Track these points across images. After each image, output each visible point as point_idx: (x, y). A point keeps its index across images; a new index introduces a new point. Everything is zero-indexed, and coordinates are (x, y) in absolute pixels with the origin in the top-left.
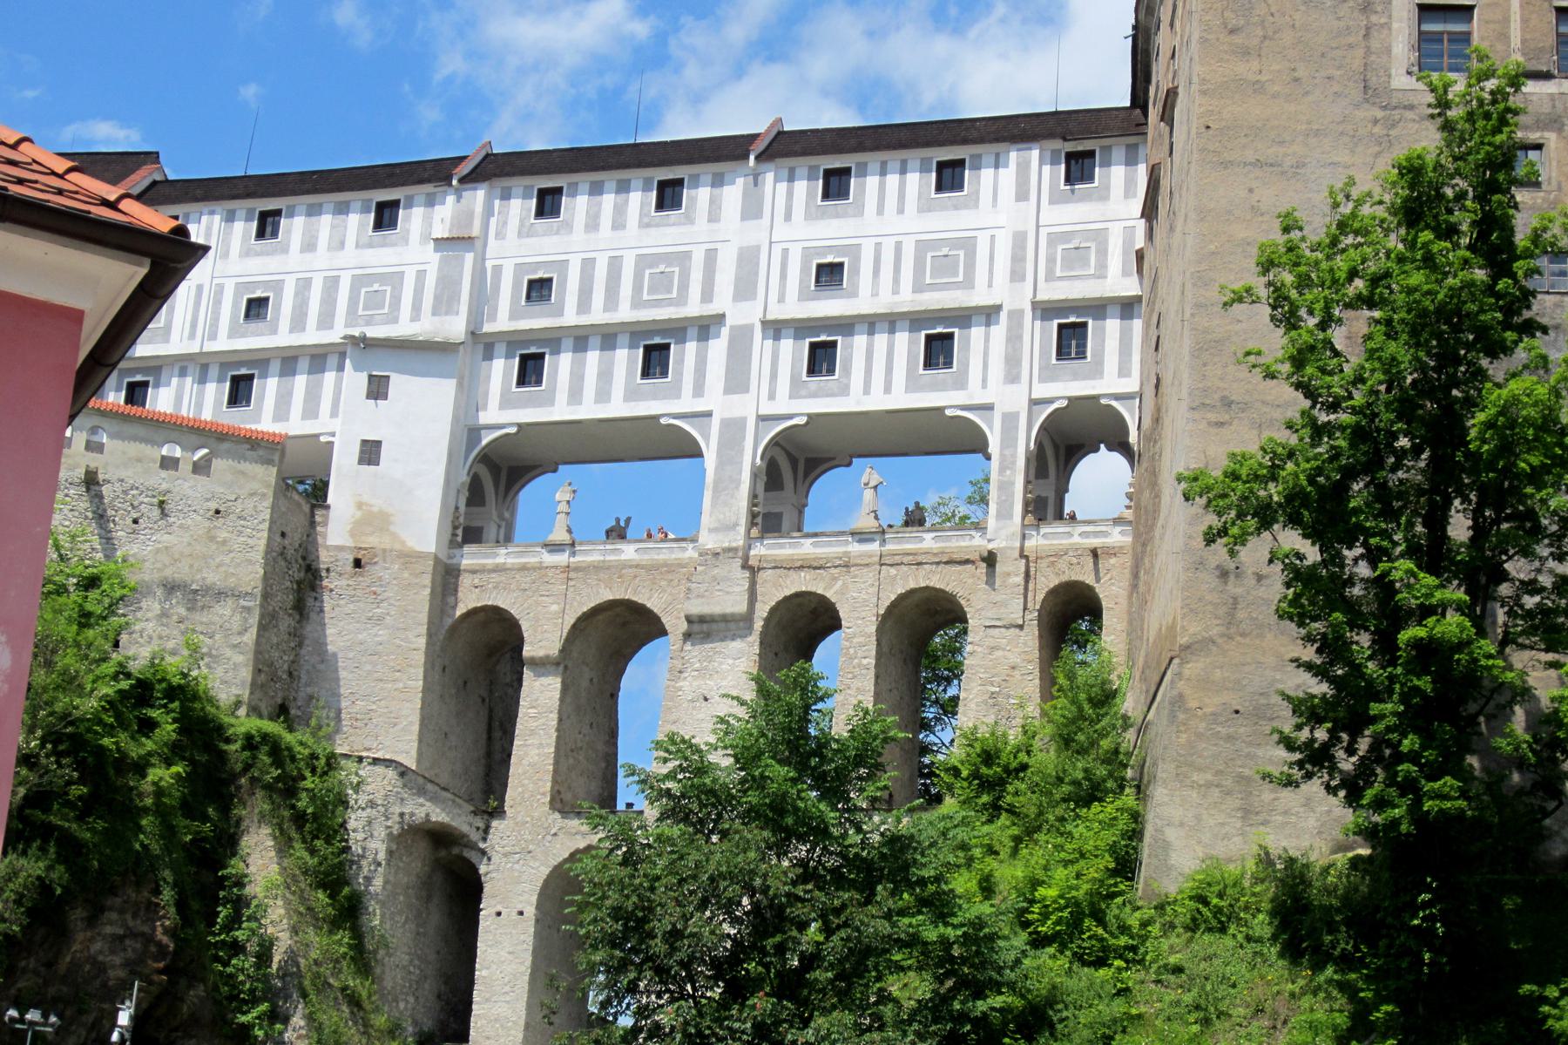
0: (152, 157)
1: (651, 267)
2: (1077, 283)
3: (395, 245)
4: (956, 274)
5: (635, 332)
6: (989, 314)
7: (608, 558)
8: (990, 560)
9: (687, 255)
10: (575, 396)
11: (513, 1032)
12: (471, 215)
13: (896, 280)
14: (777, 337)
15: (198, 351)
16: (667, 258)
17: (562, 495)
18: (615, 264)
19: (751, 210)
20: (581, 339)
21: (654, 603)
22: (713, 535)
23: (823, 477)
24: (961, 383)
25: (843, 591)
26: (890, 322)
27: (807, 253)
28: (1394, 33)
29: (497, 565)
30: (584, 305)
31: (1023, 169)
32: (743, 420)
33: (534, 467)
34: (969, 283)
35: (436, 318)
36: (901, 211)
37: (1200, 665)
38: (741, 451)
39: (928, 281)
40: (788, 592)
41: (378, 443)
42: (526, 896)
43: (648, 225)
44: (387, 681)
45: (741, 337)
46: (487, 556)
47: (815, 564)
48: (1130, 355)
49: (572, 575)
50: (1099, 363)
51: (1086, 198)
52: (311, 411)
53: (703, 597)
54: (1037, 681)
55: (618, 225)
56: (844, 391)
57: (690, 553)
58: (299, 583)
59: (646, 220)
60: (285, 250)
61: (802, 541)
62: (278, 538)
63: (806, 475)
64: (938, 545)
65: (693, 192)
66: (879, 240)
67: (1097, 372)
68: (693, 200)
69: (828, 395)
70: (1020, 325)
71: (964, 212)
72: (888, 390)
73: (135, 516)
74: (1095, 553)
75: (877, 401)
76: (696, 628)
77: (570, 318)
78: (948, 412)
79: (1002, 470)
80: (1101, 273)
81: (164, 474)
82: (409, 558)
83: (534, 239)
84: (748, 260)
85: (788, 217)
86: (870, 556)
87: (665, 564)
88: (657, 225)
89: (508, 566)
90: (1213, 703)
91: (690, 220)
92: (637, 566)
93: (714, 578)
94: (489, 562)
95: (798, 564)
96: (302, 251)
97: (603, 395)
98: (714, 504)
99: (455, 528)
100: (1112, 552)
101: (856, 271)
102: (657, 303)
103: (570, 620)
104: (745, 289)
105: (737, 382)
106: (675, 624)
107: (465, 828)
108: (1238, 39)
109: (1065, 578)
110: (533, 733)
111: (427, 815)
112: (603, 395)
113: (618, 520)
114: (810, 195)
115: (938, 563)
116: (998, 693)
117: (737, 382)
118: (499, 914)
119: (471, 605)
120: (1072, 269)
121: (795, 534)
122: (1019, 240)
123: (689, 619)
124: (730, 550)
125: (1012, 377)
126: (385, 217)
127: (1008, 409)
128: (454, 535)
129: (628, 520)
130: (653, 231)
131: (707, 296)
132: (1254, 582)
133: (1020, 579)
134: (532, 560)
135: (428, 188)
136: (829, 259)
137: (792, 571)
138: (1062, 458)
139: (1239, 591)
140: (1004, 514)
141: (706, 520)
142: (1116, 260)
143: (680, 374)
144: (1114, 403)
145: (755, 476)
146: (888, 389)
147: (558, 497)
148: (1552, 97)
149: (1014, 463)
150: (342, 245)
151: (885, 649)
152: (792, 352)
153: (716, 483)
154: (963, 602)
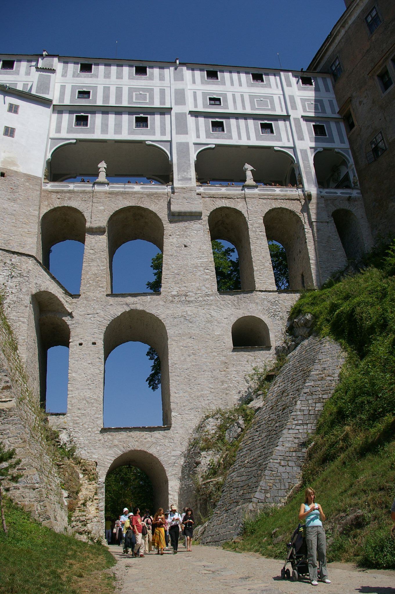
5: (130, 111)
7: (126, 190)
11: (94, 405)
14: (196, 117)
22: (180, 182)
26: (246, 117)
29: (70, 190)
32: (187, 144)
33: (67, 175)
39: (257, 107)
42: (96, 335)
43: (132, 79)
44: (19, 228)
47: (228, 197)
49: (109, 195)
57: (167, 189)
61: (221, 188)
65: (151, 70)
66: (234, 93)
69: (223, 138)
71: (265, 89)
75: (244, 142)
76: (176, 218)
82: (29, 178)
83: (80, 79)
85: (194, 82)
87: (156, 193)
88: (136, 79)
89: (76, 191)
92: (142, 194)
93: (184, 198)
94: (65, 189)
95: (221, 196)
100: (355, 200)
101: (226, 101)
105: (182, 129)
107: (61, 299)
109: (339, 208)
110: (93, 260)
112: (118, 130)
114: (202, 77)
115: (283, 199)
118: (81, 344)
119: (56, 206)
121: (217, 185)
137: (217, 199)
143: (153, 128)
146: (249, 138)
149: (310, 166)
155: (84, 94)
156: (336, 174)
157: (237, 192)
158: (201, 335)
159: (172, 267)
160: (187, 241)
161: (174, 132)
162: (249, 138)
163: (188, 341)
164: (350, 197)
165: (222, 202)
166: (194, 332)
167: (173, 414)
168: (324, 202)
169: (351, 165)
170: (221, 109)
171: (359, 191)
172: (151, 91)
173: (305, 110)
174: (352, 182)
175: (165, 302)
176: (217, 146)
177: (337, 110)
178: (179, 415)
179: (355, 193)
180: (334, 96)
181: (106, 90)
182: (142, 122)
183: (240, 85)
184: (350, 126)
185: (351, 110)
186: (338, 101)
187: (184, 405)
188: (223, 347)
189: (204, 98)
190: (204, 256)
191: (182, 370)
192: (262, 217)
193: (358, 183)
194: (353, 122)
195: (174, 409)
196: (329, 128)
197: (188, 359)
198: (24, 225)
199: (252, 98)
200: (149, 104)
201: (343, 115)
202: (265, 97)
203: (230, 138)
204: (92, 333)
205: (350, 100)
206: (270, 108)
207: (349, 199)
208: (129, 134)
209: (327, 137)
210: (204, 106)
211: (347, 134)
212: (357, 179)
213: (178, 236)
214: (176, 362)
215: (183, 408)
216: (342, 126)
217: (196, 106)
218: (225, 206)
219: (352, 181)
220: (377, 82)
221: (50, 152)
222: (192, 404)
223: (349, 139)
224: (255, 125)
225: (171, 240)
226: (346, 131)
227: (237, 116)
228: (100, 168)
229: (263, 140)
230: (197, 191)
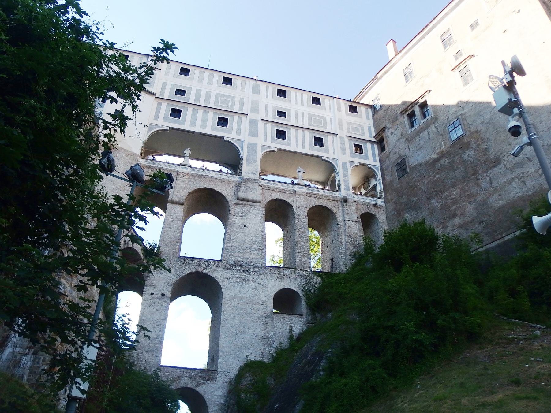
10: (193, 123)
27: (274, 107)
32: (255, 145)
38: (256, 152)
40: (274, 198)
42: (165, 288)
45: (253, 123)
46: (154, 164)
47: (282, 191)
48: (375, 157)
51: (355, 116)
53: (245, 192)
57: (237, 178)
59: (219, 85)
66: (297, 110)
69: (284, 145)
70: (344, 141)
76: (241, 202)
85: (267, 97)
86: (303, 193)
88: (223, 87)
89: (164, 169)
93: (249, 187)
95: (277, 190)
97: (204, 125)
105: (253, 133)
112: (204, 125)
116: (353, 240)
117: (253, 133)
118: (152, 294)
123: (238, 199)
124: (255, 180)
133: (355, 208)
144: (372, 167)
146: (304, 147)
152: (271, 130)
153: (247, 160)
154: (334, 212)
155: (181, 92)
156: (367, 184)
158: (249, 299)
159: (233, 242)
160: (246, 222)
161: (247, 133)
162: (304, 147)
163: (238, 302)
164: (376, 204)
165: (278, 194)
166: (244, 296)
167: (220, 360)
168: (355, 205)
169: (380, 179)
171: (383, 200)
172: (233, 98)
173: (349, 132)
174: (378, 192)
175: (224, 269)
176: (280, 150)
177: (374, 134)
178: (225, 362)
179: (380, 202)
180: (372, 123)
181: (198, 92)
182: (223, 122)
183: (303, 105)
184: (382, 149)
185: (384, 137)
186: (375, 127)
187: (230, 354)
188: (265, 311)
189: (273, 110)
190: (258, 236)
191: (231, 325)
192: (306, 211)
193: (383, 194)
194: (384, 146)
195: (221, 356)
196: (366, 148)
197: (237, 317)
198: (121, 191)
199: (310, 116)
200: (230, 109)
201: (377, 140)
202: (320, 117)
203: (290, 145)
204: (162, 286)
205: (383, 130)
206: (323, 126)
207: (375, 205)
208: (212, 129)
209: (364, 154)
210: (272, 117)
211: (379, 155)
212: (383, 191)
213: (240, 217)
214: (226, 318)
215: (228, 357)
216: (376, 146)
217: (266, 116)
218: (279, 198)
219: (378, 192)
220: (406, 120)
221: (147, 134)
222: (236, 354)
223: (380, 158)
225: (235, 220)
226: (379, 153)
228: (185, 153)
230: (259, 183)
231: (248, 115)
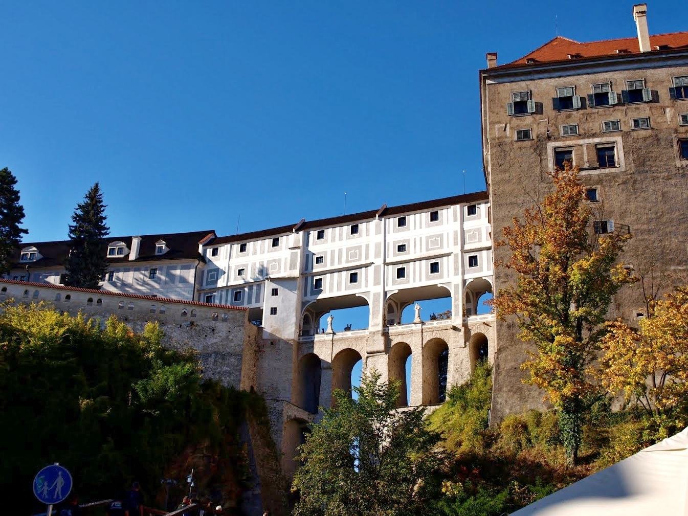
0: (213, 232)
1: (351, 251)
2: (473, 244)
3: (279, 251)
4: (438, 245)
5: (347, 269)
6: (448, 255)
8: (455, 328)
9: (361, 246)
10: (331, 290)
12: (299, 240)
13: (421, 248)
15: (225, 286)
16: (355, 248)
17: (329, 319)
18: (340, 251)
19: (378, 232)
20: (332, 272)
21: (357, 349)
23: (406, 308)
24: (441, 277)
25: (411, 341)
26: (420, 259)
27: (395, 243)
28: (549, 161)
30: (332, 263)
31: (455, 212)
32: (379, 294)
34: (442, 247)
35: (291, 271)
36: (421, 228)
37: (504, 355)
41: (275, 309)
43: (349, 239)
46: (309, 339)
50: (481, 268)
51: (475, 218)
52: (258, 300)
54: (470, 364)
55: (341, 239)
56: (408, 282)
57: (366, 332)
58: (255, 351)
60: (248, 255)
62: (248, 338)
63: (401, 307)
64: (439, 325)
67: (481, 270)
68: (361, 230)
70: (458, 258)
72: (420, 280)
73: (205, 334)
74: (484, 323)
77: (329, 268)
78: (439, 286)
79: (455, 301)
80: (480, 240)
81: (213, 322)
84: (377, 246)
85: (389, 233)
90: (508, 366)
91: (361, 236)
96: (253, 255)
97: (339, 289)
98: (373, 318)
99: (300, 331)
101: (409, 246)
102: (353, 261)
103: (334, 356)
104: (377, 255)
106: (364, 355)
107: (307, 419)
108: (502, 167)
111: (295, 416)
112: (339, 289)
113: (348, 325)
117: (376, 283)
120: (472, 240)
122: (455, 233)
124: (379, 331)
125: (456, 274)
126: (275, 243)
127: (456, 283)
128: (299, 333)
129: (351, 325)
130: (351, 240)
131: (367, 258)
132: (518, 328)
134: (322, 339)
135: (287, 233)
136: (401, 244)
138: (475, 298)
139: (514, 331)
140: (457, 314)
141: (371, 323)
142: (484, 235)
145: (384, 309)
146: (420, 280)
147: (328, 320)
148: (598, 175)
149: (458, 299)
150: (264, 252)
151: (425, 357)
153: (373, 312)
157: (409, 329)
170: (406, 254)
202: (437, 236)
224: (426, 265)
227: (414, 260)
229: (430, 279)
231: (372, 263)
